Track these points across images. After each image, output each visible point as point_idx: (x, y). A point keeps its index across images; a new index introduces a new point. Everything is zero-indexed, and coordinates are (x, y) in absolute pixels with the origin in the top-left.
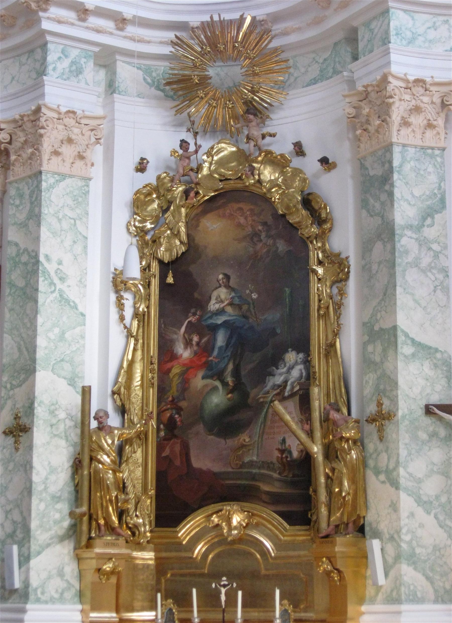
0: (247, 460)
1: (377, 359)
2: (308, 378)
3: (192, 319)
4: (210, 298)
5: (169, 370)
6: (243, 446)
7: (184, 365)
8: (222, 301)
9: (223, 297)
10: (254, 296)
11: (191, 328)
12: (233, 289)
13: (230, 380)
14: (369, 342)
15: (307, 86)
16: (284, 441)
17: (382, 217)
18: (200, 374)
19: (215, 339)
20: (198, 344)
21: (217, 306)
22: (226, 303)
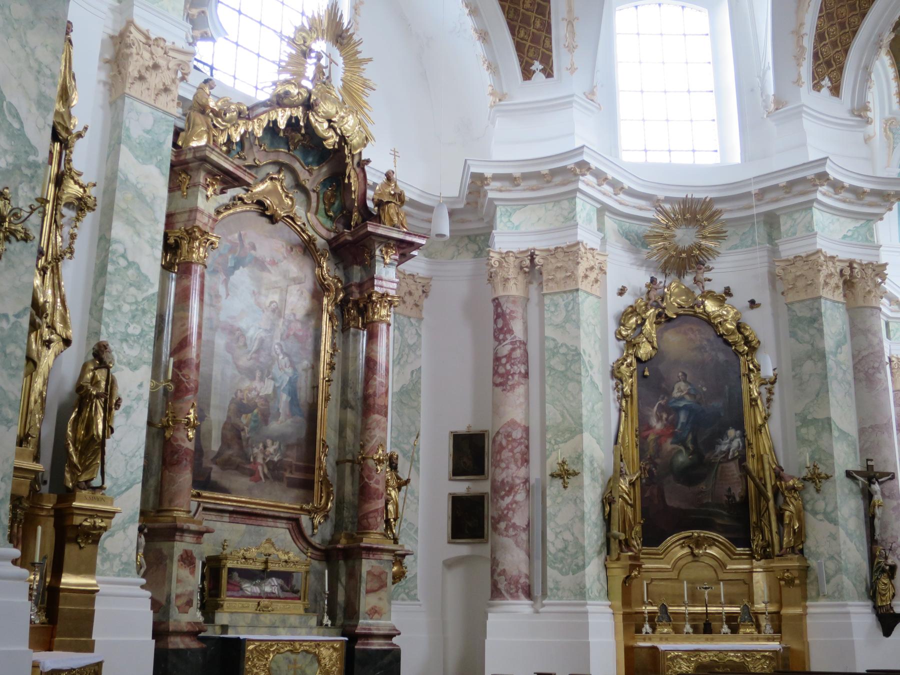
0: (705, 501)
1: (812, 438)
2: (744, 447)
3: (662, 402)
4: (673, 389)
5: (647, 436)
6: (702, 492)
7: (657, 434)
8: (682, 391)
9: (682, 388)
10: (704, 389)
11: (662, 408)
12: (690, 384)
13: (690, 446)
14: (802, 426)
15: (730, 249)
16: (729, 490)
17: (812, 345)
18: (669, 440)
19: (679, 418)
20: (667, 419)
21: (679, 394)
22: (685, 392)
